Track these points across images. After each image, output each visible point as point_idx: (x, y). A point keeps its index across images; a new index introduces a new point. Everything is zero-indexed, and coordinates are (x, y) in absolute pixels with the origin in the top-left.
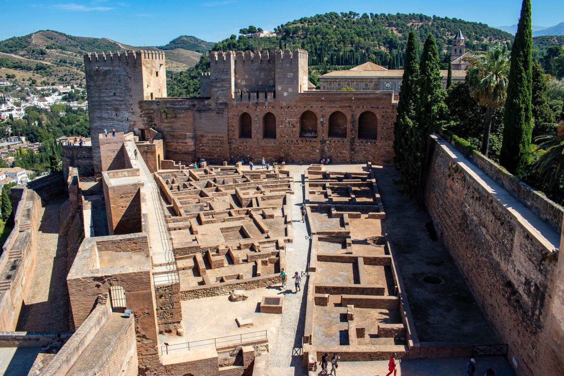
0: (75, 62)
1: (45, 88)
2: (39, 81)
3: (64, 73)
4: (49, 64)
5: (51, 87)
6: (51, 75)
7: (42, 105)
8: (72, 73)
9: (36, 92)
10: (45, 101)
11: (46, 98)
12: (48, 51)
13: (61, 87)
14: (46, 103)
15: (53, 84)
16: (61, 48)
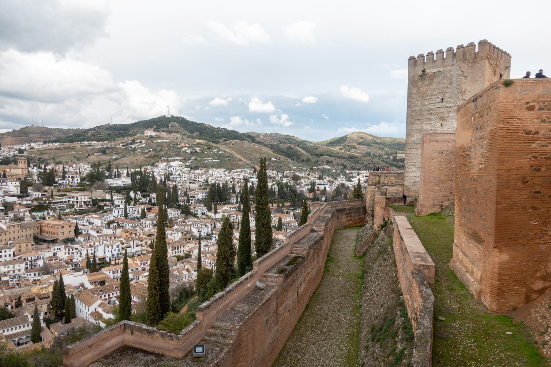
0: (378, 155)
1: (352, 171)
2: (348, 166)
3: (368, 162)
4: (357, 155)
5: (357, 171)
6: (358, 163)
7: (348, 184)
8: (374, 162)
9: (345, 174)
10: (351, 181)
11: (352, 179)
12: (358, 146)
13: (365, 172)
14: (352, 183)
15: (359, 169)
16: (368, 145)
